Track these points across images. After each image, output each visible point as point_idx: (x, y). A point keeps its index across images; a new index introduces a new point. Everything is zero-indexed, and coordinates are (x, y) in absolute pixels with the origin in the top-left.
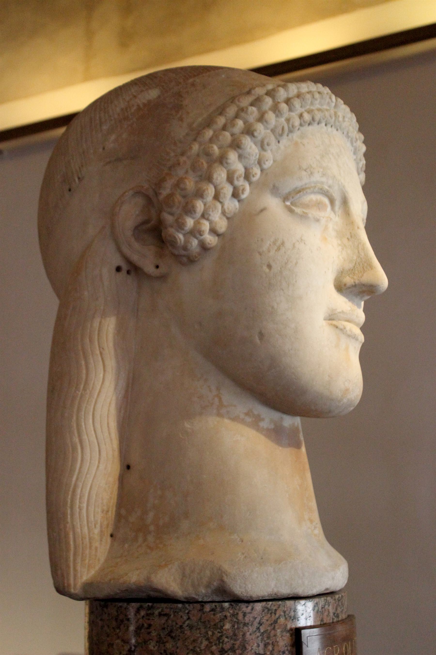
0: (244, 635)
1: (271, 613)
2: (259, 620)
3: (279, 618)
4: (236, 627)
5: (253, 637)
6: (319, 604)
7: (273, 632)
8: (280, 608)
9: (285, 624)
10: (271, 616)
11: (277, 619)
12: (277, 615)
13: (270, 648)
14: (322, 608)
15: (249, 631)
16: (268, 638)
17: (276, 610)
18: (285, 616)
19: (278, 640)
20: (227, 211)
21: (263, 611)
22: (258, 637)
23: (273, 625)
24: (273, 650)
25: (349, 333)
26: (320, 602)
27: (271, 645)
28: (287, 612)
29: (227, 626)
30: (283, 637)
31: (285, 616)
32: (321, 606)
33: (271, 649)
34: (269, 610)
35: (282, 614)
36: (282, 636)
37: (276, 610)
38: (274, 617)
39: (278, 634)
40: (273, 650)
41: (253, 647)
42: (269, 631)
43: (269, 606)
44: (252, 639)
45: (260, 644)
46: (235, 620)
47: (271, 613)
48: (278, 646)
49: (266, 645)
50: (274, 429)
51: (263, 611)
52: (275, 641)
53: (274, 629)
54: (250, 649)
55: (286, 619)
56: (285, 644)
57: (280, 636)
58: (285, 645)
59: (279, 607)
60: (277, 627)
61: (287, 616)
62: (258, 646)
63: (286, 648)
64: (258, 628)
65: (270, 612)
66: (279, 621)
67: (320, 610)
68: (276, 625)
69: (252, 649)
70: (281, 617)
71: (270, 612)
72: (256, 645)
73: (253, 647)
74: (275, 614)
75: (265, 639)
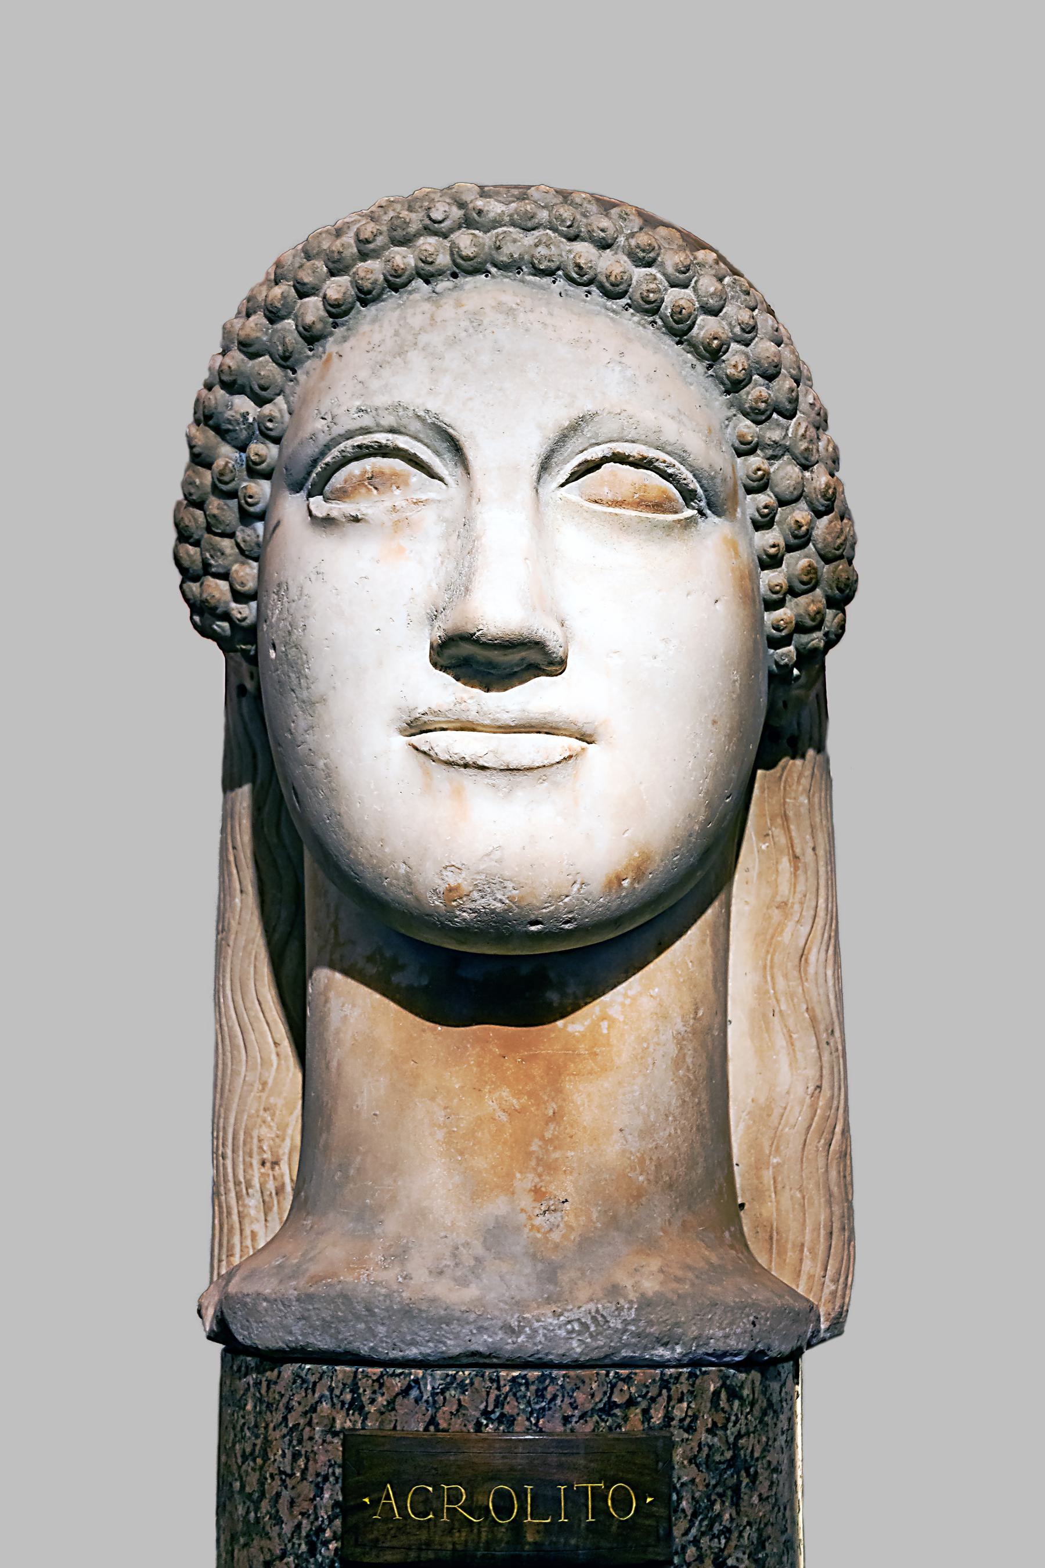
0: (266, 1428)
1: (306, 1389)
2: (287, 1400)
3: (320, 1401)
4: (258, 1409)
5: (278, 1434)
6: (426, 1385)
7: (308, 1429)
8: (323, 1381)
9: (331, 1417)
10: (306, 1396)
11: (317, 1403)
12: (317, 1395)
13: (301, 1463)
14: (434, 1394)
15: (272, 1421)
16: (300, 1442)
17: (315, 1384)
18: (332, 1398)
19: (316, 1448)
20: (242, 545)
21: (294, 1382)
22: (284, 1436)
23: (309, 1416)
24: (306, 1468)
25: (444, 757)
26: (429, 1379)
27: (303, 1457)
28: (337, 1392)
29: (249, 1407)
30: (325, 1445)
31: (332, 1398)
32: (429, 1388)
33: (303, 1466)
34: (304, 1381)
35: (327, 1393)
36: (324, 1441)
37: (315, 1384)
38: (312, 1399)
39: (317, 1437)
40: (306, 1468)
41: (277, 1457)
42: (300, 1428)
43: (303, 1374)
44: (276, 1440)
45: (286, 1451)
46: (258, 1395)
47: (306, 1389)
48: (316, 1461)
49: (296, 1456)
50: (427, 986)
51: (294, 1383)
52: (310, 1450)
53: (310, 1423)
54: (272, 1459)
55: (333, 1405)
56: (329, 1461)
57: (320, 1441)
58: (328, 1463)
59: (320, 1379)
60: (315, 1421)
61: (335, 1400)
62: (284, 1455)
63: (331, 1470)
64: (285, 1419)
65: (305, 1386)
66: (319, 1409)
67: (425, 1397)
68: (314, 1415)
69: (275, 1460)
70: (323, 1399)
71: (305, 1386)
72: (280, 1452)
73: (277, 1457)
74: (314, 1392)
75: (295, 1443)
